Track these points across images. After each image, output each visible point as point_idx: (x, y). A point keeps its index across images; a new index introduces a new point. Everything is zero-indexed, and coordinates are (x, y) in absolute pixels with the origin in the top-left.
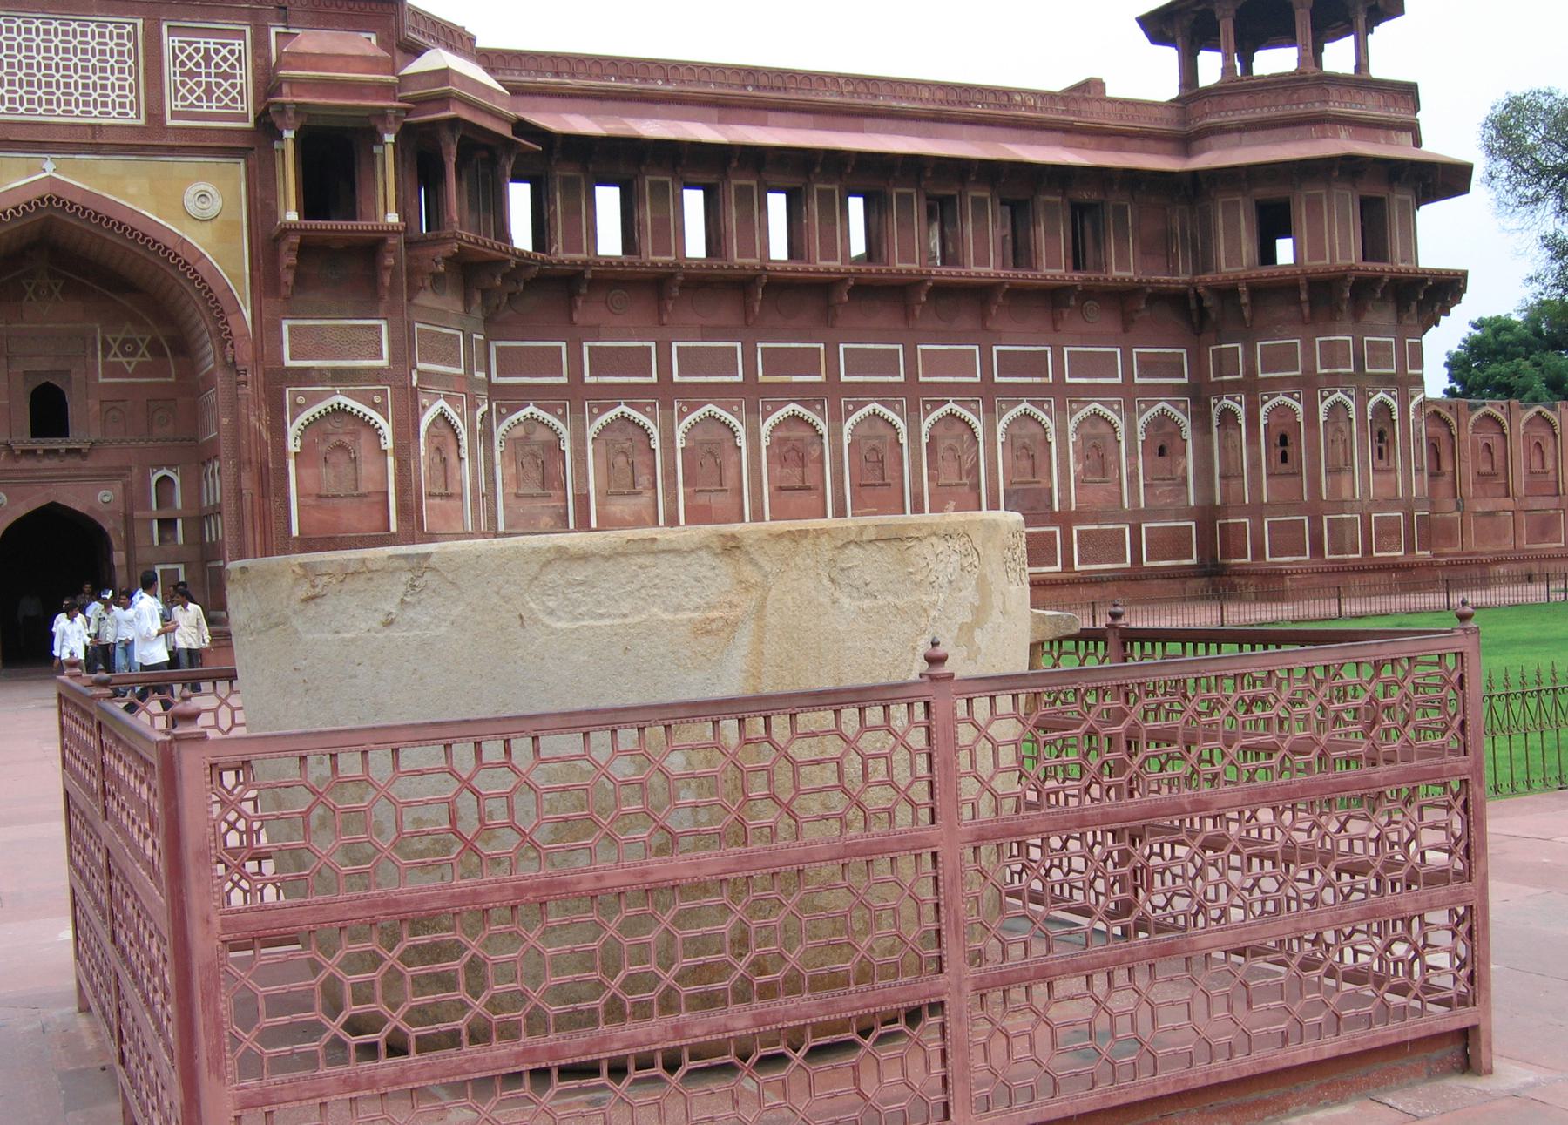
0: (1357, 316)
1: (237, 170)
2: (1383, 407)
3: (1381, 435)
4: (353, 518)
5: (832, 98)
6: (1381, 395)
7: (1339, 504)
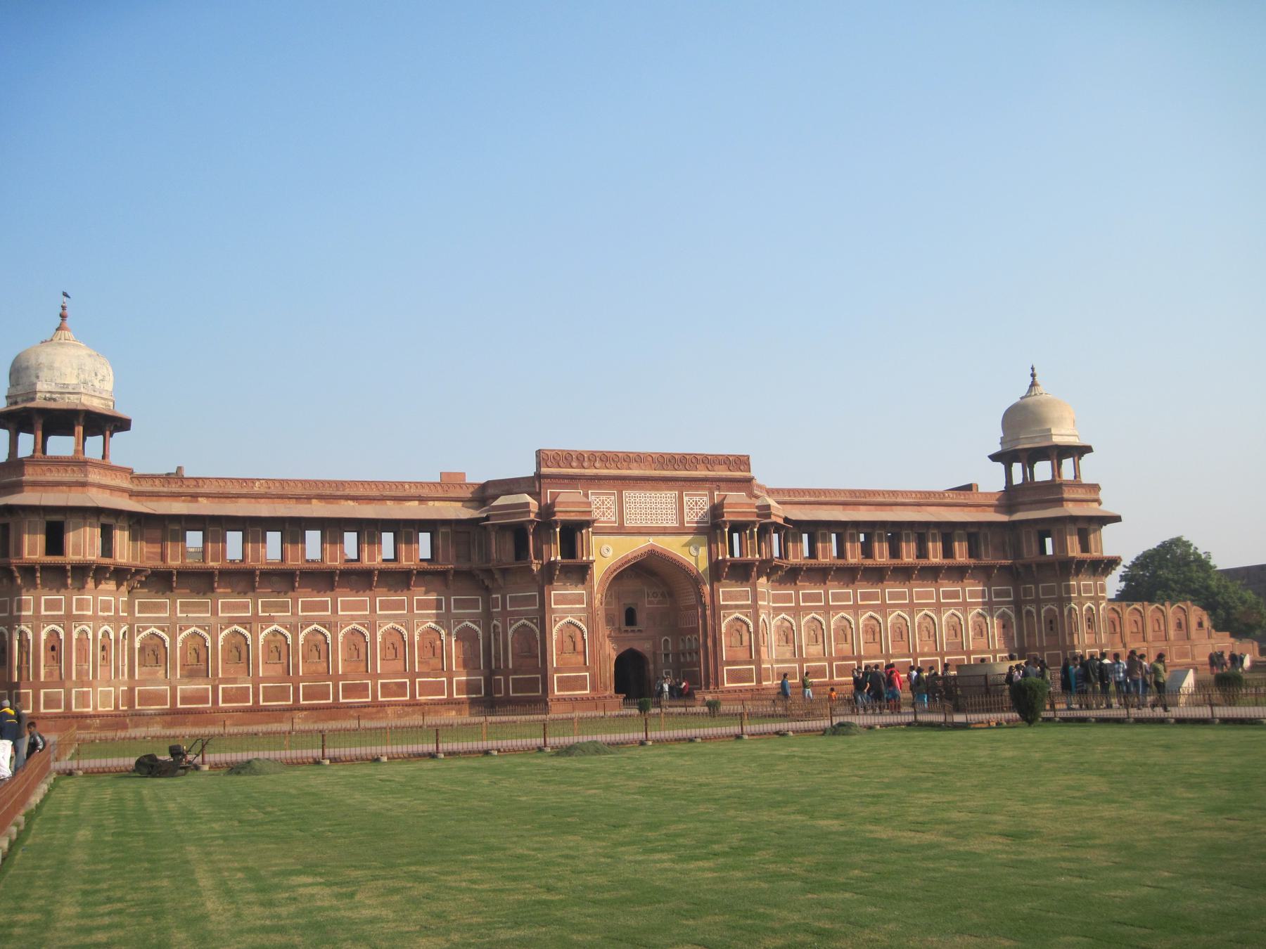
0: (1077, 575)
1: (704, 538)
2: (1090, 608)
3: (1091, 622)
4: (743, 655)
5: (880, 499)
6: (1089, 604)
7: (1073, 647)
